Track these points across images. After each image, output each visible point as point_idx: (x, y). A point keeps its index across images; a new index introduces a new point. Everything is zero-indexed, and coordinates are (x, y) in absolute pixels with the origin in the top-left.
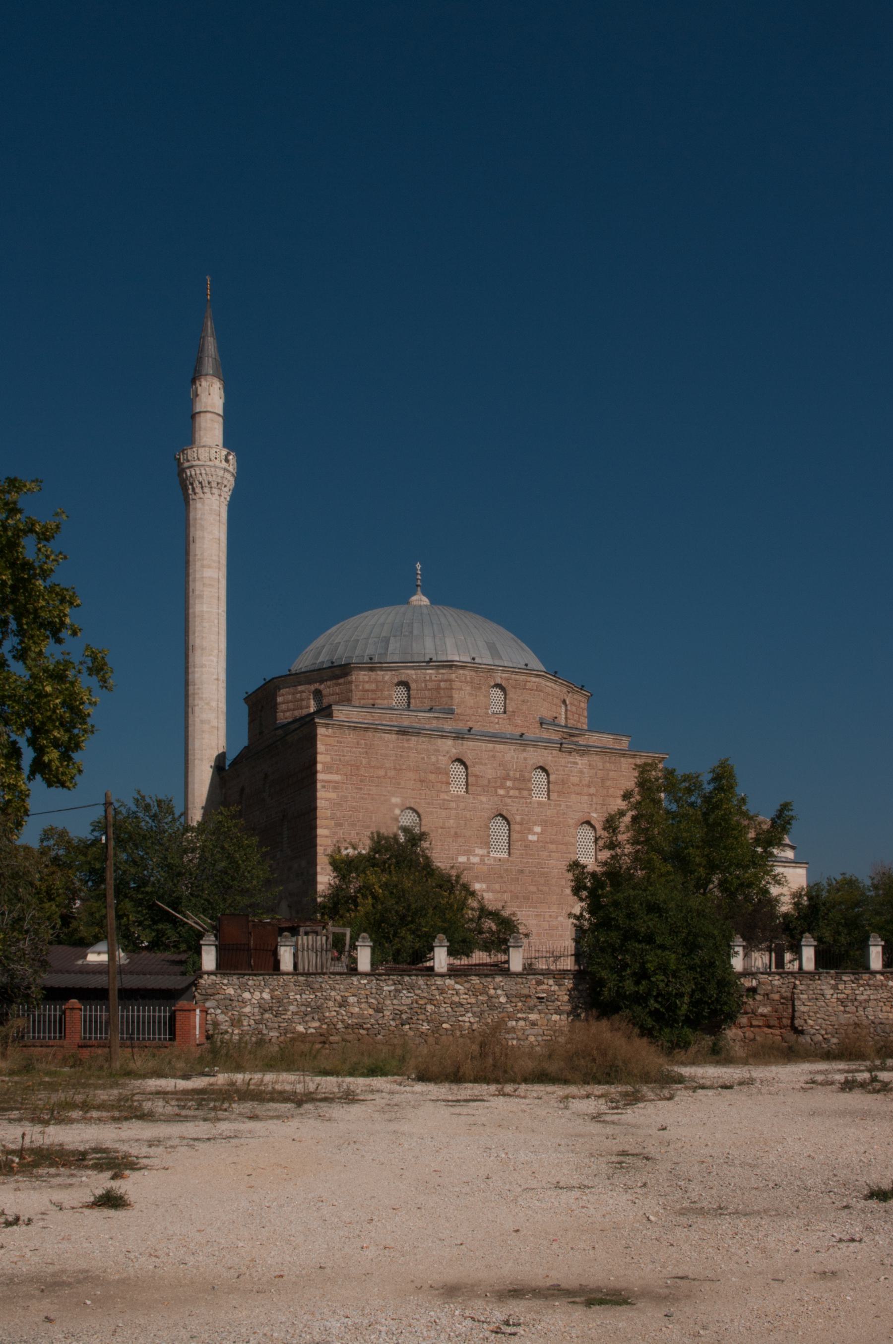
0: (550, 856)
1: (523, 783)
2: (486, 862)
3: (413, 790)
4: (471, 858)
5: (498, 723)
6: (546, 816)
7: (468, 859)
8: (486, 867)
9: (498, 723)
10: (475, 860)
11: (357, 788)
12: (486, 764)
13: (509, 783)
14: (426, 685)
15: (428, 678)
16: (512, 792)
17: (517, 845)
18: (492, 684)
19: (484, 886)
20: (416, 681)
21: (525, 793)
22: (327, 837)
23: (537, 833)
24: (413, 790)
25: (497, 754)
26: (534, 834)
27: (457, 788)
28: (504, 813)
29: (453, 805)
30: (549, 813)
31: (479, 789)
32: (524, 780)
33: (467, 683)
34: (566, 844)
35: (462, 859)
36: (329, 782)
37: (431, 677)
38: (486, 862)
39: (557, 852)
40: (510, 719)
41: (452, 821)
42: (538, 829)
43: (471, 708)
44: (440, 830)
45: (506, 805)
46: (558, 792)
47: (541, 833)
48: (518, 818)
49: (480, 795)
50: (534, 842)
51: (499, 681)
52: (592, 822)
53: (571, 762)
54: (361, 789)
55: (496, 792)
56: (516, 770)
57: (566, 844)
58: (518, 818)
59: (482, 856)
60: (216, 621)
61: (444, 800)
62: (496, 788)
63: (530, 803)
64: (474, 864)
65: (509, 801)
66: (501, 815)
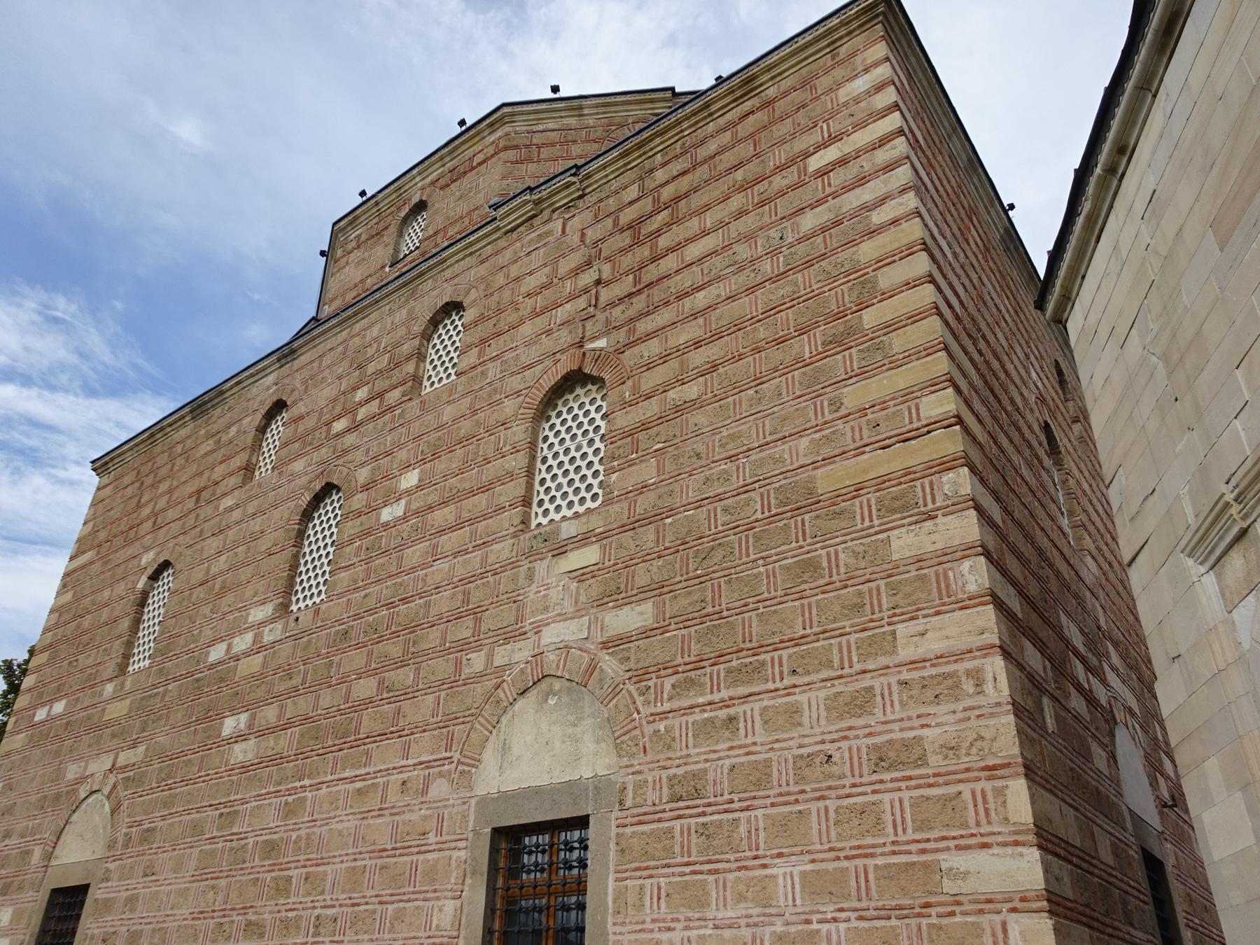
35: (217, 653)
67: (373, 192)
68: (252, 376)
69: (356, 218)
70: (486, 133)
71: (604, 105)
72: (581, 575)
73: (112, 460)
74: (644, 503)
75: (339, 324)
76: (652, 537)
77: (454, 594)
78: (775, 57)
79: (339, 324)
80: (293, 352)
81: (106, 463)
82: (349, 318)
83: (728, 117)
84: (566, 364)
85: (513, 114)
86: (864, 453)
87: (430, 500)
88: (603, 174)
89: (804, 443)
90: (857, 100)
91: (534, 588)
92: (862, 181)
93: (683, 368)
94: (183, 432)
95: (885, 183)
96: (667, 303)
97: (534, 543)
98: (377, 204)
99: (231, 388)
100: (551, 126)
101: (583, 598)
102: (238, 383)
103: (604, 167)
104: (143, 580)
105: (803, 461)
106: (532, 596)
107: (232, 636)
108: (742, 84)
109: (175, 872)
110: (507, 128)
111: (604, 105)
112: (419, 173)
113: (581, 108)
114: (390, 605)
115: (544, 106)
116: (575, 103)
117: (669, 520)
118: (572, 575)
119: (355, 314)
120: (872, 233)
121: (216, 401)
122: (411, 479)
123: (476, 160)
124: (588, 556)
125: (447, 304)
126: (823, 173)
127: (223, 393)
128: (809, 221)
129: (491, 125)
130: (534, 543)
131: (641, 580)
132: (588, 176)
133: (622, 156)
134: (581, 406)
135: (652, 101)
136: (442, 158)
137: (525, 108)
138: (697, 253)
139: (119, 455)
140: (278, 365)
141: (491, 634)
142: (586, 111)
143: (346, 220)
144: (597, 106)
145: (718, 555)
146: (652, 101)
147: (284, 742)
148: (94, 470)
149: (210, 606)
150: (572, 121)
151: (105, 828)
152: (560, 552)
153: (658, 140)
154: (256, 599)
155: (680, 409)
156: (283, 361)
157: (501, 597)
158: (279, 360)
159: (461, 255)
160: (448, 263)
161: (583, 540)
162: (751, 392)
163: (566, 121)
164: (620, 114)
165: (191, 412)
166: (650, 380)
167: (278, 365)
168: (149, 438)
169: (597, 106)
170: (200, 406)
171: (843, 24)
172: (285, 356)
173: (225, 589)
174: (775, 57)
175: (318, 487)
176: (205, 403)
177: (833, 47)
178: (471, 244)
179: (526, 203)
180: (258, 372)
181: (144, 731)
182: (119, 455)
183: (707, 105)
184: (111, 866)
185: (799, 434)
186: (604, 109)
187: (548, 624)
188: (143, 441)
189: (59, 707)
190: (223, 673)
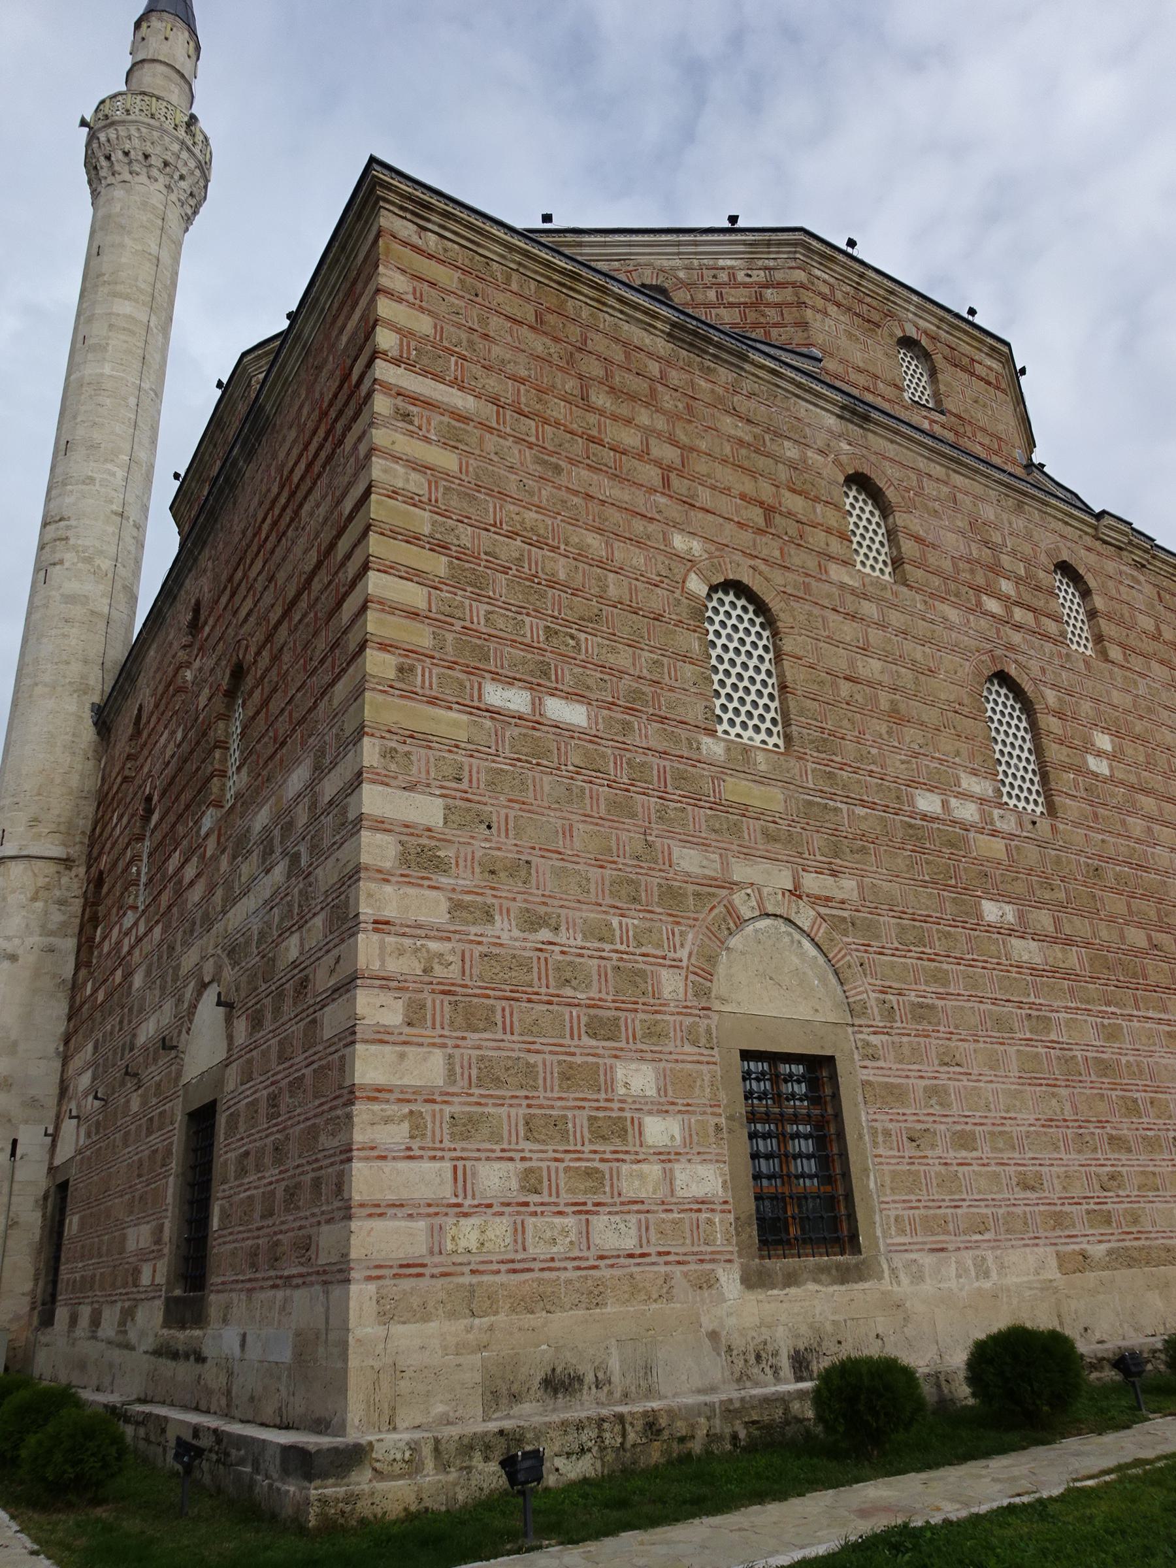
14: (720, 295)
15: (723, 277)
17: (1064, 780)
19: (1010, 913)
20: (689, 286)
22: (414, 615)
27: (871, 561)
28: (1012, 670)
36: (428, 404)
37: (732, 276)
48: (1051, 696)
60: (132, 401)
66: (1002, 678)
67: (860, 257)
68: (799, 385)
69: (832, 259)
73: (446, 215)
75: (931, 450)
79: (931, 450)
80: (866, 418)
81: (428, 207)
98: (862, 276)
99: (762, 367)
102: (773, 372)
109: (991, 1068)
119: (952, 459)
121: (725, 356)
127: (744, 358)
129: (993, 348)
136: (942, 320)
139: (470, 227)
143: (823, 248)
147: (1073, 958)
151: (824, 981)
156: (847, 415)
159: (1060, 515)
160: (1049, 510)
165: (674, 325)
167: (837, 411)
168: (562, 272)
170: (695, 334)
172: (854, 412)
176: (709, 341)
178: (1071, 516)
180: (810, 391)
182: (470, 227)
184: (874, 1039)
189: (567, 712)
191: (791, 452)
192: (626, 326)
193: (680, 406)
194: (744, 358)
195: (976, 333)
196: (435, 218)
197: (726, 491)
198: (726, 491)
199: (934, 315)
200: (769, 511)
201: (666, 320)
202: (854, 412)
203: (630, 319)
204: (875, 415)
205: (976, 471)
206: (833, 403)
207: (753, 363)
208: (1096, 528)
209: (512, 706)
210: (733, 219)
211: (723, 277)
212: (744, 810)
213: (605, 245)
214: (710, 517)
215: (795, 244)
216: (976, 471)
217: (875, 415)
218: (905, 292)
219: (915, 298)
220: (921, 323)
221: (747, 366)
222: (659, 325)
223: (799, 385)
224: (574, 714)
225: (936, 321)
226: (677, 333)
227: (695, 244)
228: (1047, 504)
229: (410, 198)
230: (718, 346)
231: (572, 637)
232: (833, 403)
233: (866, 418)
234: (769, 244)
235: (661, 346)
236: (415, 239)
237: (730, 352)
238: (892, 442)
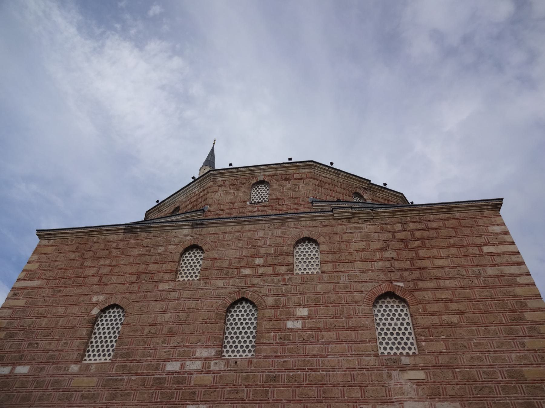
0: (327, 349)
1: (280, 259)
2: (212, 368)
3: (124, 284)
4: (188, 363)
5: (258, 211)
6: (317, 293)
7: (182, 366)
8: (210, 377)
9: (258, 211)
10: (196, 365)
11: (54, 291)
12: (228, 245)
13: (258, 261)
16: (261, 271)
18: (254, 181)
21: (283, 269)
23: (303, 318)
24: (124, 284)
25: (244, 234)
26: (297, 319)
29: (175, 295)
30: (320, 288)
31: (216, 272)
32: (281, 255)
33: (225, 186)
34: (354, 329)
35: (172, 367)
38: (212, 368)
39: (340, 342)
40: (272, 206)
41: (167, 316)
42: (304, 312)
43: (227, 203)
44: (147, 329)
45: (253, 286)
46: (334, 262)
47: (309, 317)
49: (216, 279)
50: (297, 330)
51: (261, 178)
52: (398, 293)
53: (351, 228)
54: (60, 291)
55: (239, 272)
56: (270, 245)
57: (354, 329)
58: (270, 301)
59: (206, 359)
61: (164, 290)
62: (239, 268)
63: (290, 279)
64: (191, 373)
65: (256, 281)
70: (301, 168)
71: (347, 177)
72: (418, 383)
73: (55, 234)
74: (442, 360)
75: (234, 222)
76: (451, 375)
77: (345, 375)
78: (460, 205)
80: (203, 224)
82: (242, 222)
83: (440, 216)
84: (385, 288)
85: (315, 166)
86: (540, 367)
87: (318, 325)
88: (383, 214)
89: (513, 356)
90: (497, 234)
91: (393, 382)
92: (508, 264)
93: (447, 308)
94: (116, 237)
95: (520, 269)
96: (431, 279)
97: (388, 362)
98: (237, 172)
99: (157, 227)
100: (327, 176)
101: (421, 393)
103: (385, 212)
104: (95, 311)
105: (515, 363)
106: (392, 386)
107: (185, 359)
108: (447, 208)
110: (311, 170)
111: (347, 177)
112: (264, 169)
113: (339, 174)
114: (303, 370)
115: (326, 168)
116: (338, 172)
117: (457, 370)
118: (413, 381)
120: (520, 285)
121: (143, 230)
122: (304, 312)
123: (296, 176)
124: (420, 375)
125: (306, 237)
126: (491, 255)
127: (151, 227)
128: (490, 271)
130: (388, 362)
131: (451, 391)
132: (377, 213)
133: (393, 212)
134: (402, 311)
135: (363, 182)
136: (277, 168)
137: (320, 166)
138: (441, 264)
140: (190, 227)
141: (371, 398)
142: (340, 176)
144: (345, 176)
145: (487, 391)
146: (363, 182)
148: (38, 235)
149: (162, 339)
150: (335, 178)
152: (403, 369)
153: (409, 212)
154: (199, 344)
155: (450, 324)
156: (195, 226)
157: (374, 382)
158: (192, 225)
161: (415, 367)
162: (483, 328)
163: (332, 176)
164: (352, 182)
165: (125, 229)
166: (432, 308)
167: (190, 227)
168: (88, 232)
169: (345, 176)
170: (132, 228)
171: (486, 205)
172: (197, 225)
173: (171, 333)
174: (460, 205)
175: (237, 298)
176: (137, 228)
177: (482, 211)
178: (316, 216)
179: (349, 212)
180: (177, 226)
181: (113, 399)
183: (431, 209)
185: (511, 351)
186: (345, 178)
187: (406, 401)
188: (84, 232)
189: (22, 370)
190: (180, 379)
191: (161, 249)
192: (109, 237)
193: (119, 253)
194: (151, 227)
195: (294, 165)
196: (53, 236)
197: (125, 274)
198: (125, 274)
199: (274, 168)
200: (139, 274)
201: (122, 229)
202: (197, 225)
203: (111, 234)
204: (205, 222)
205: (259, 220)
206: (188, 225)
207: (154, 227)
208: (333, 215)
209: (3, 373)
210: (193, 178)
211: (197, 192)
212: (77, 389)
213: (169, 201)
214: (112, 286)
215: (210, 175)
216: (261, 220)
217: (205, 222)
218: (257, 168)
219: (262, 167)
220: (267, 173)
221: (152, 229)
222: (120, 231)
223: (172, 226)
224: (22, 370)
225: (275, 170)
226: (126, 231)
227: (188, 189)
228: (301, 217)
229: (46, 235)
230: (141, 228)
231: (37, 344)
232: (188, 225)
233: (203, 224)
234: (203, 179)
235: (121, 236)
236: (47, 244)
237: (145, 228)
238: (216, 227)
